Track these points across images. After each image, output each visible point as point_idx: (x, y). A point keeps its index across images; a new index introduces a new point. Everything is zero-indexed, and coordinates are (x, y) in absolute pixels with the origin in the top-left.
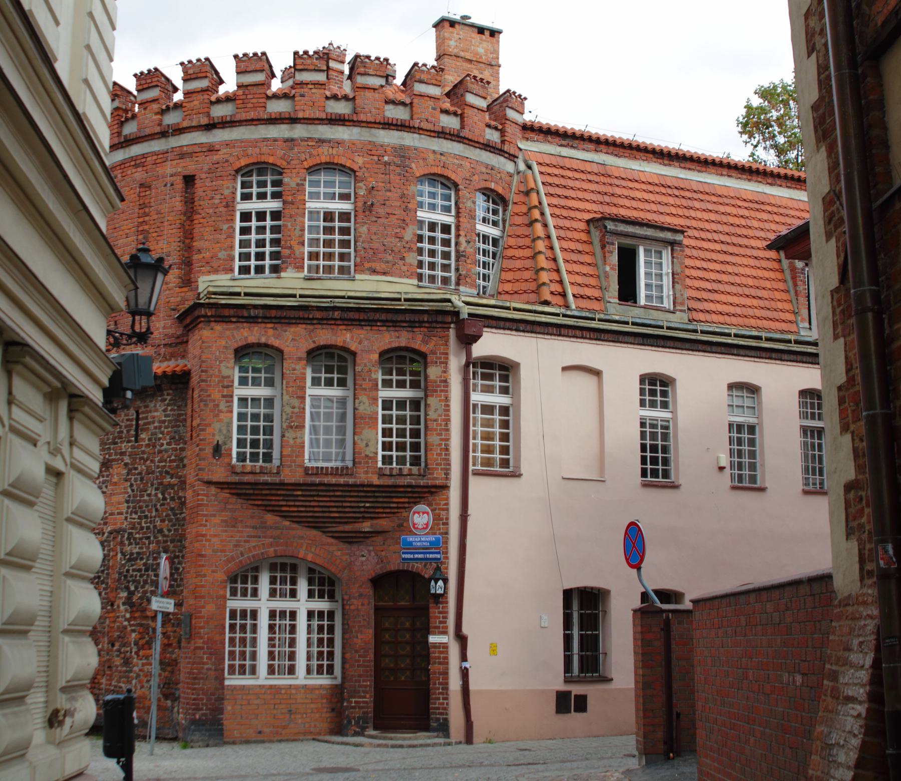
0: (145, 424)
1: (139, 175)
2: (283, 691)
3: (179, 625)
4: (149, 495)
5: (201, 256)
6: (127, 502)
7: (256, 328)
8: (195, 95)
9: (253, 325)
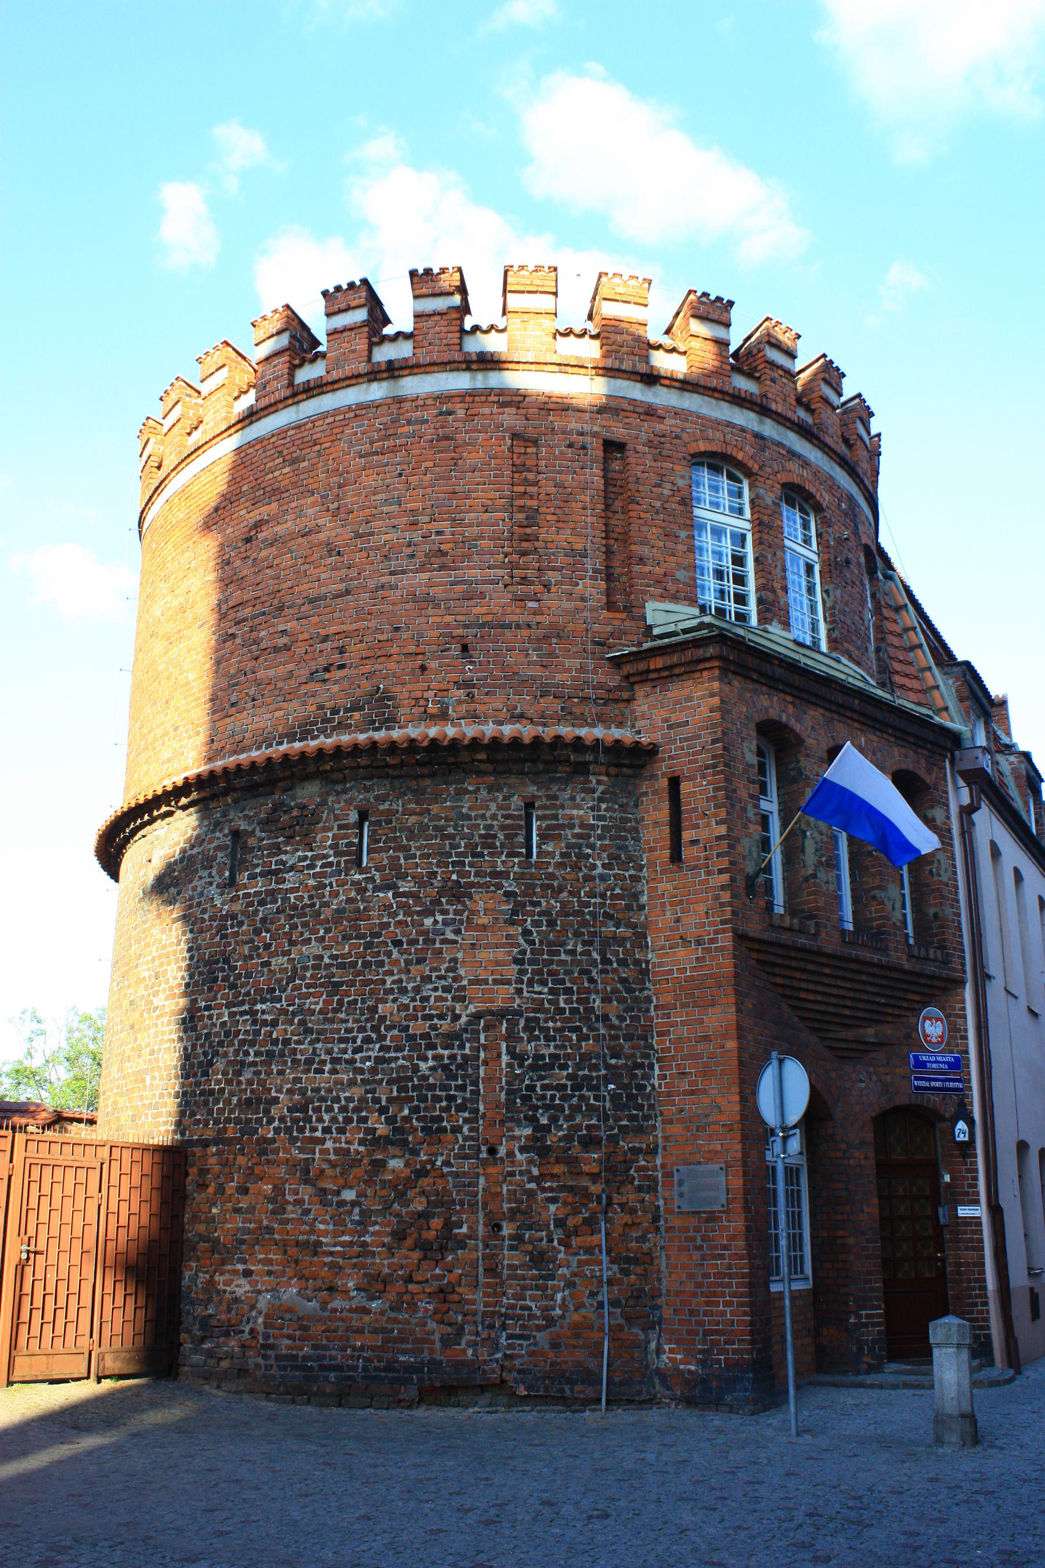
0: (548, 827)
1: (509, 418)
3: (653, 1189)
4: (572, 952)
5: (647, 569)
6: (517, 961)
9: (773, 692)
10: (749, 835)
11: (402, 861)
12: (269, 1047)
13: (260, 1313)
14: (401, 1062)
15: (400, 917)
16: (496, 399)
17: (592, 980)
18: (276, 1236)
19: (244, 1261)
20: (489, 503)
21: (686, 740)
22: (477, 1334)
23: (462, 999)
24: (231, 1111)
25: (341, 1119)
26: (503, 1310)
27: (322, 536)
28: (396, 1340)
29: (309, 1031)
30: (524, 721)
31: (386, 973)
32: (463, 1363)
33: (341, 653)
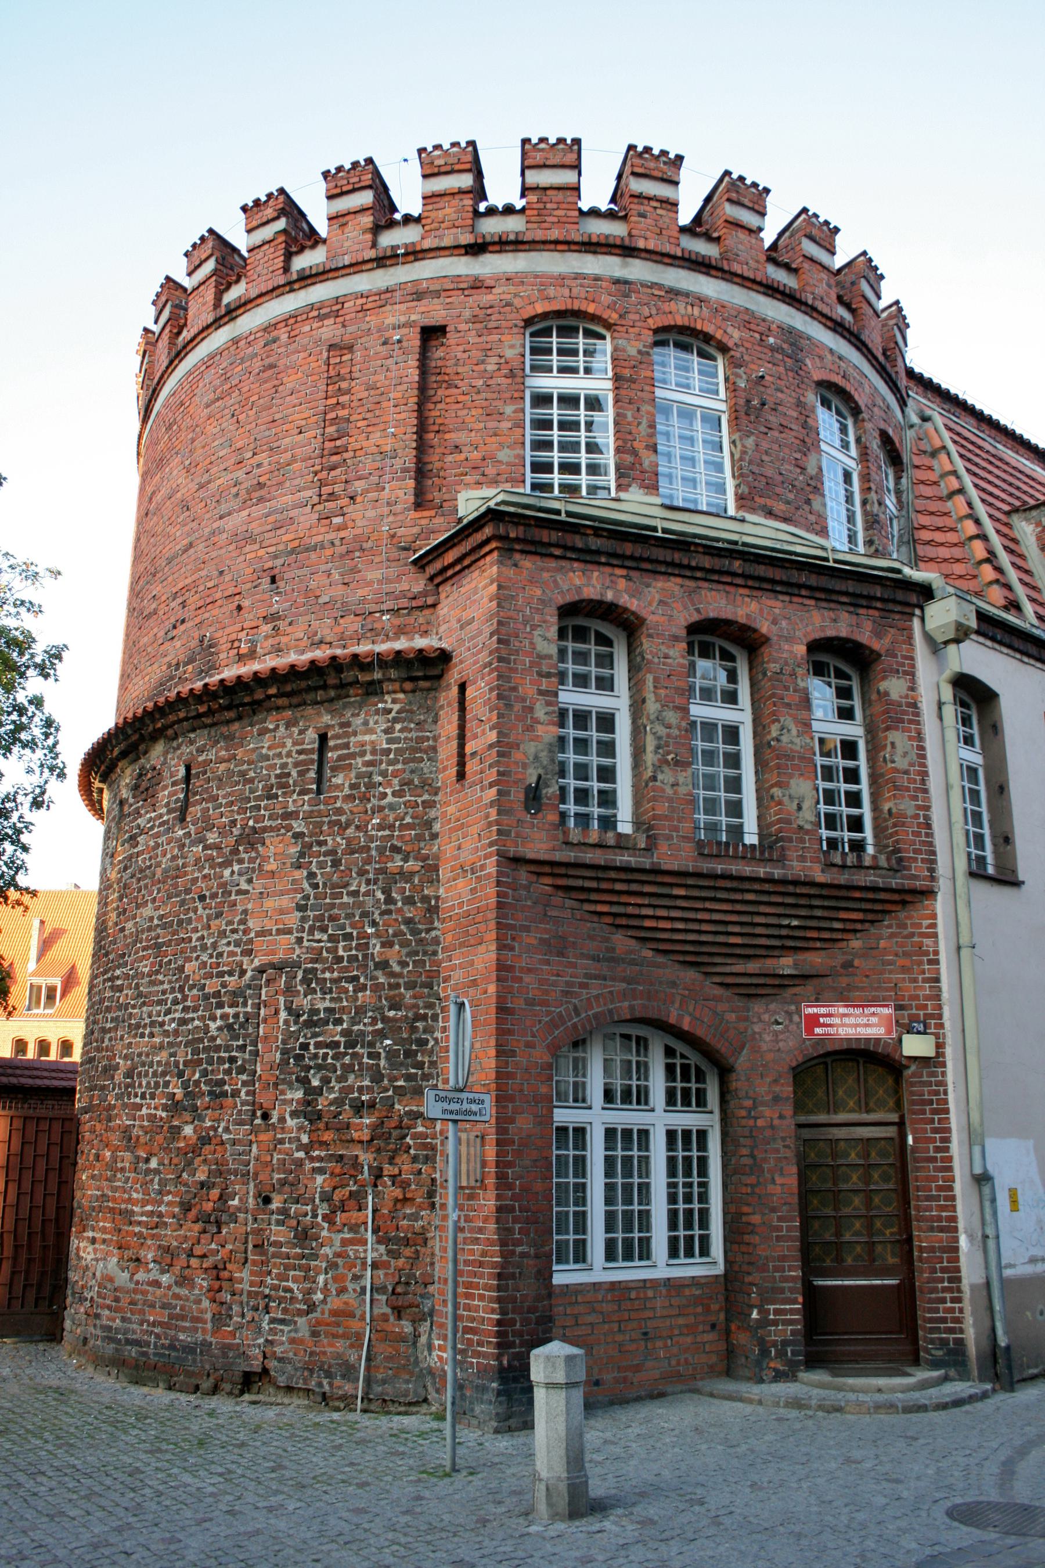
0: (340, 758)
1: (329, 331)
2: (633, 1295)
4: (355, 894)
5: (463, 456)
6: (301, 908)
7: (596, 574)
8: (446, 198)
9: (589, 566)
10: (536, 739)
14: (197, 1023)
15: (206, 871)
16: (316, 313)
20: (303, 423)
26: (267, 1291)
30: (323, 646)
32: (230, 1347)
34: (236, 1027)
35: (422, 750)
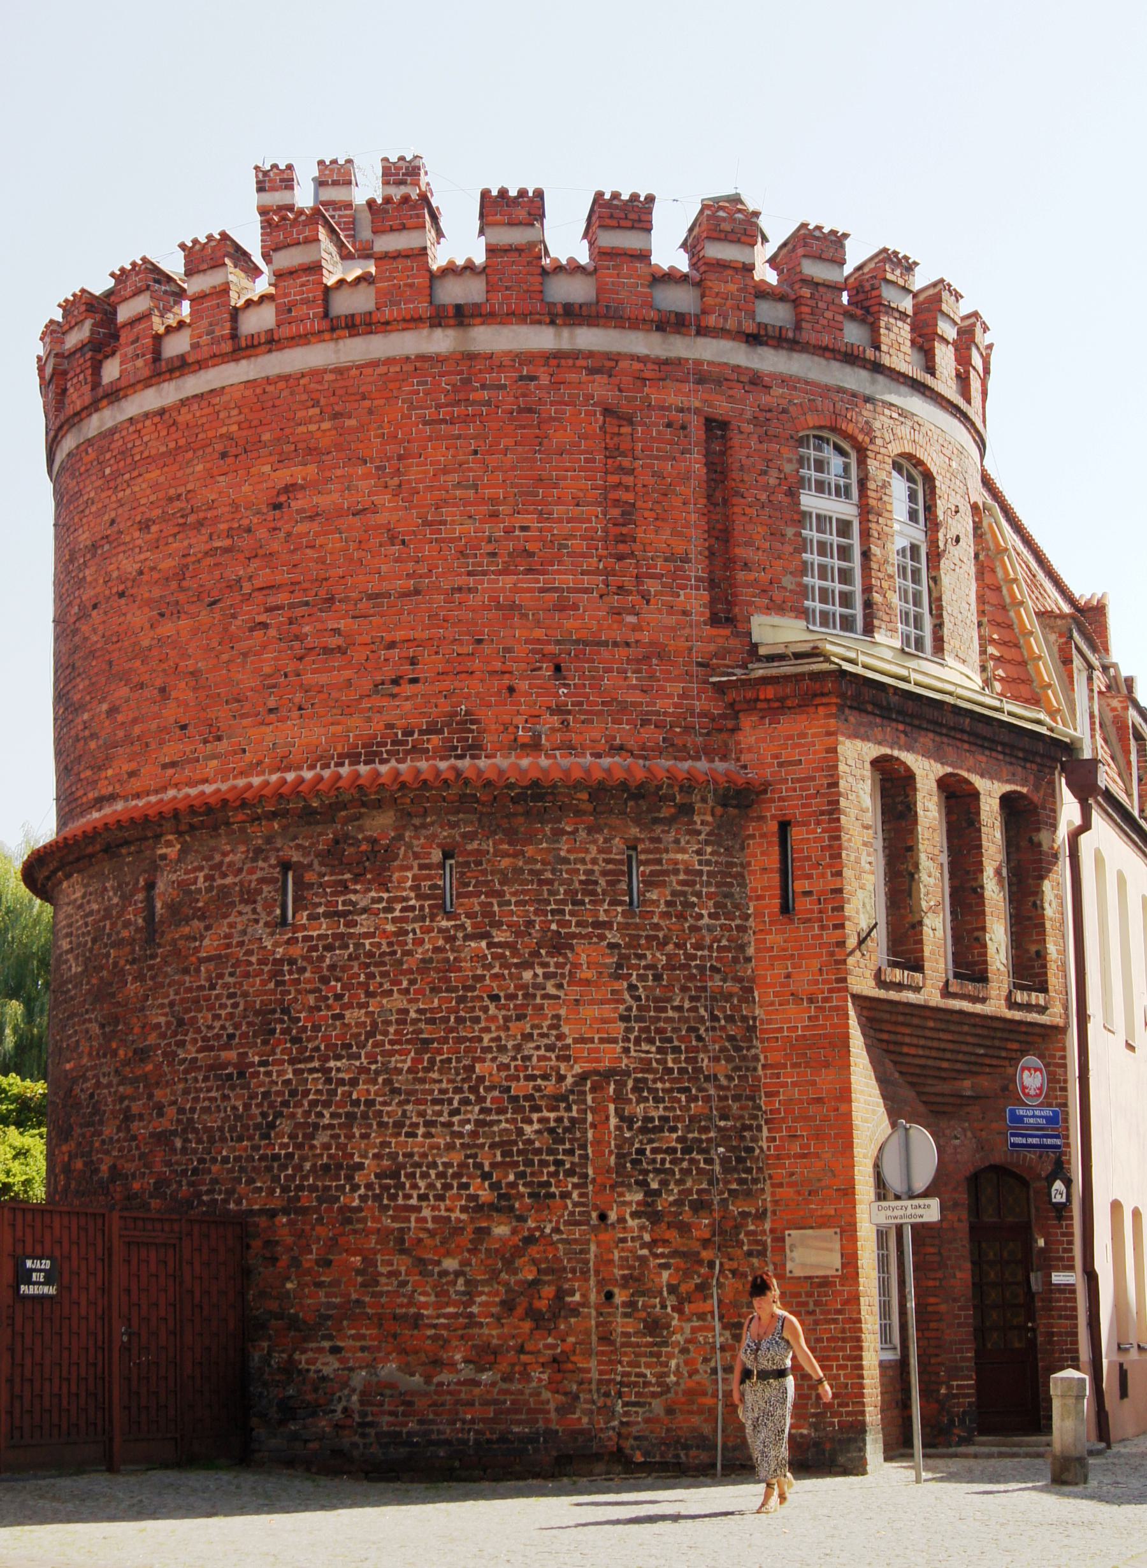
0: (652, 873)
1: (600, 388)
3: (762, 1254)
4: (679, 1009)
6: (625, 1019)
8: (730, 272)
9: (885, 722)
11: (496, 908)
12: (349, 1109)
13: (354, 1390)
14: (504, 1125)
15: (496, 970)
17: (700, 1038)
18: (369, 1311)
19: (329, 1337)
21: (799, 780)
22: (593, 1402)
23: (567, 1059)
24: (305, 1178)
25: (439, 1186)
26: (618, 1378)
27: (382, 518)
28: (508, 1411)
29: (395, 1091)
31: (483, 1030)
32: (582, 1432)
33: (413, 664)
34: (560, 1131)
35: (729, 877)
